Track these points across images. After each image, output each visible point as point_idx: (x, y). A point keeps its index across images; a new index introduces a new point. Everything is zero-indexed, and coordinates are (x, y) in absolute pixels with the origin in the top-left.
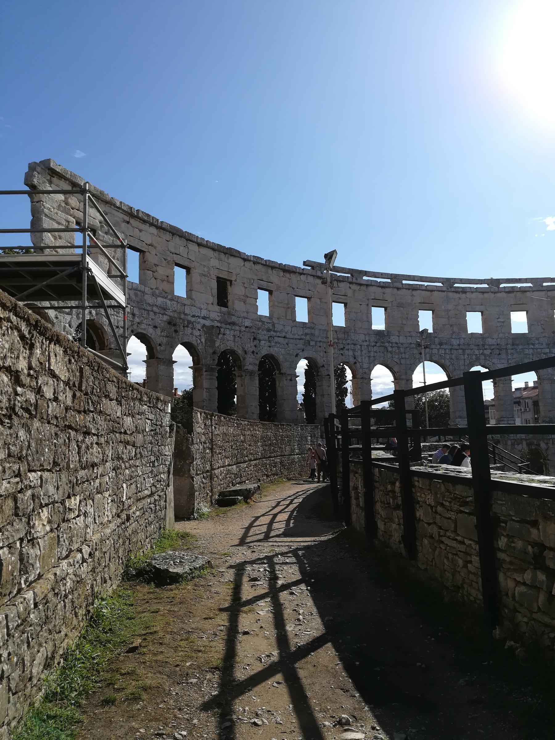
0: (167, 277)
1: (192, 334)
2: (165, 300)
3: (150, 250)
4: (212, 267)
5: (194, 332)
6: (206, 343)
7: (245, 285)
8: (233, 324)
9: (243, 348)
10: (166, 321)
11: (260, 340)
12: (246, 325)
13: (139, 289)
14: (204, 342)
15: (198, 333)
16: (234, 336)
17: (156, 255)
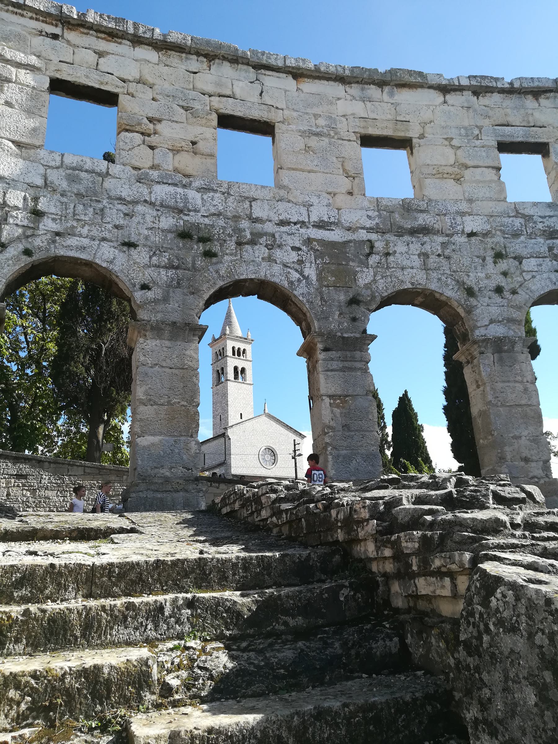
0: (194, 143)
1: (270, 259)
2: (180, 190)
3: (131, 90)
4: (344, 116)
5: (278, 254)
6: (320, 278)
7: (455, 142)
8: (425, 230)
9: (460, 284)
10: (170, 231)
11: (519, 259)
12: (468, 230)
13: (86, 167)
14: (314, 277)
15: (294, 257)
16: (425, 256)
17: (153, 99)
